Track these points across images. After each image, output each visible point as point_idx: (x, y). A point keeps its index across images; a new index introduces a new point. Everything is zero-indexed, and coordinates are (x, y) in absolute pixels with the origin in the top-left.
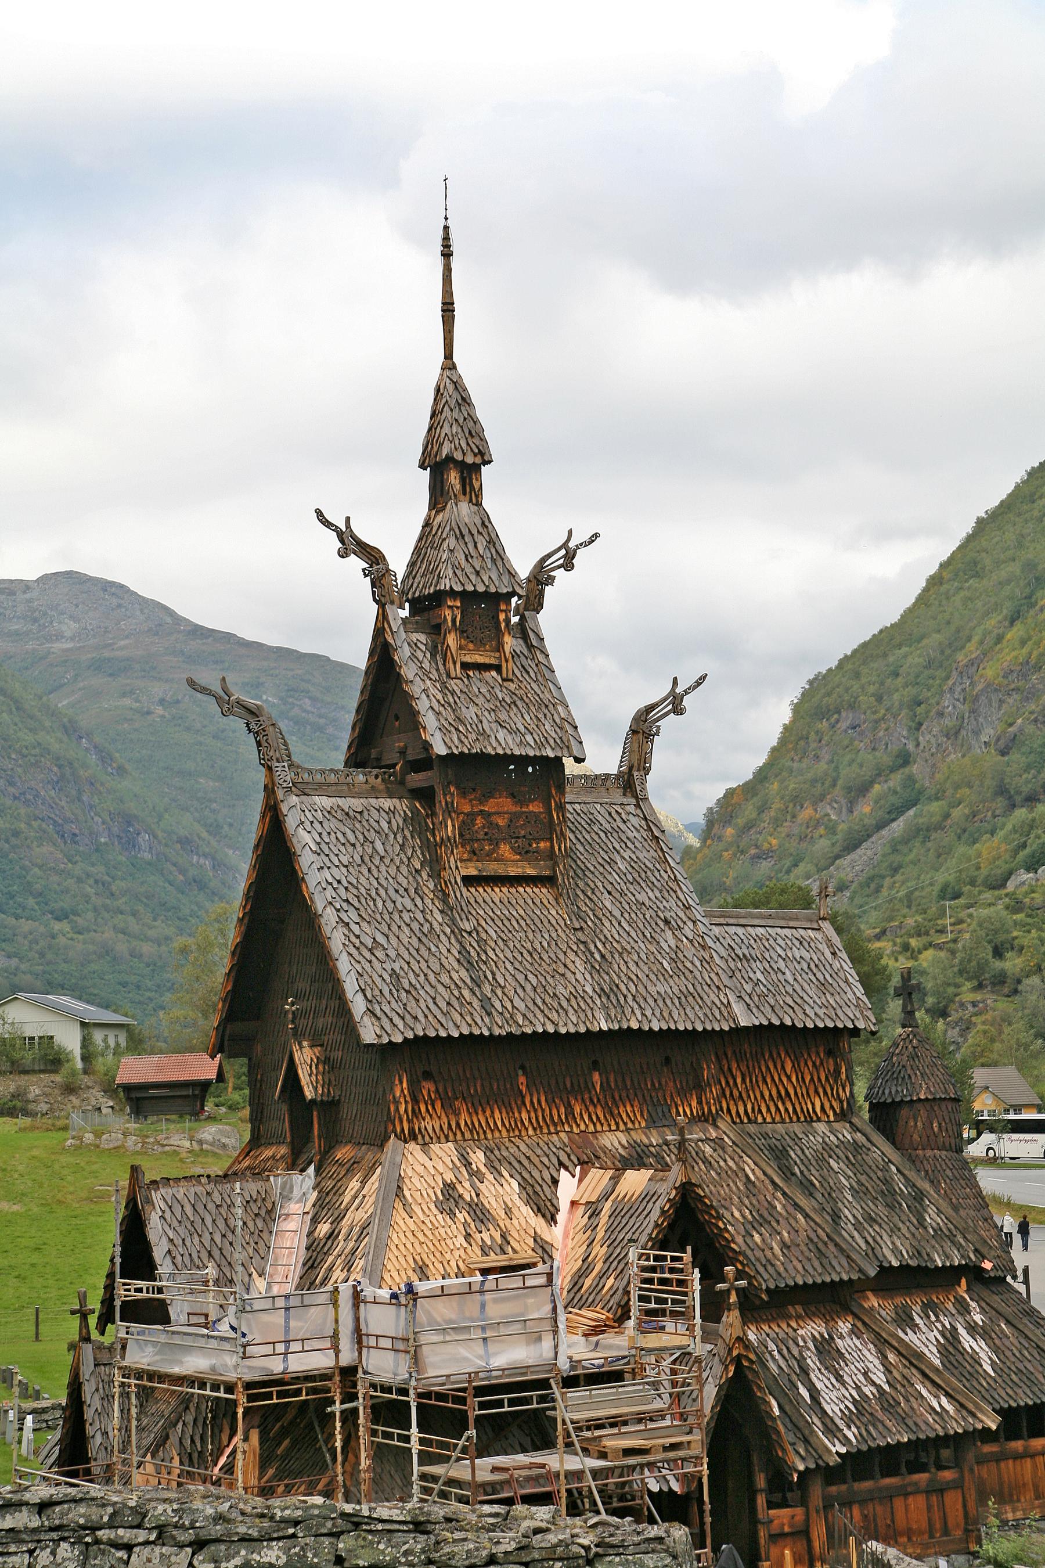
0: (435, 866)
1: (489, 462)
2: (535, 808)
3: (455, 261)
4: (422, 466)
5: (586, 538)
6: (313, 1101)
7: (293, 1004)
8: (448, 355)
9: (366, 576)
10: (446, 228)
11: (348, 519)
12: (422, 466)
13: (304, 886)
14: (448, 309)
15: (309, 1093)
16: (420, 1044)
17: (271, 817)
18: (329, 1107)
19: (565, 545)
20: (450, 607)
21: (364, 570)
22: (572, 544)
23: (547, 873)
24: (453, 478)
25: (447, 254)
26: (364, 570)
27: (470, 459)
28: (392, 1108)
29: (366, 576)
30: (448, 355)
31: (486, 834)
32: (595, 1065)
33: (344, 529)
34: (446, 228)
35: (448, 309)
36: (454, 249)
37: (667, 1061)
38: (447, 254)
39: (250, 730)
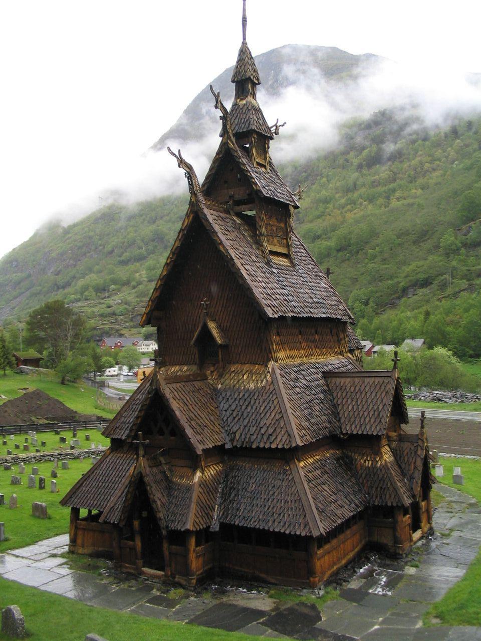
0: (259, 244)
1: (259, 84)
2: (282, 225)
4: (233, 81)
5: (282, 124)
6: (221, 345)
7: (205, 301)
8: (244, 39)
9: (221, 119)
13: (221, 247)
14: (244, 20)
15: (219, 341)
16: (282, 318)
17: (193, 217)
18: (224, 347)
19: (276, 125)
20: (254, 137)
22: (278, 125)
23: (287, 253)
28: (271, 347)
29: (221, 119)
30: (244, 39)
32: (316, 332)
35: (244, 20)
37: (331, 332)
39: (186, 176)
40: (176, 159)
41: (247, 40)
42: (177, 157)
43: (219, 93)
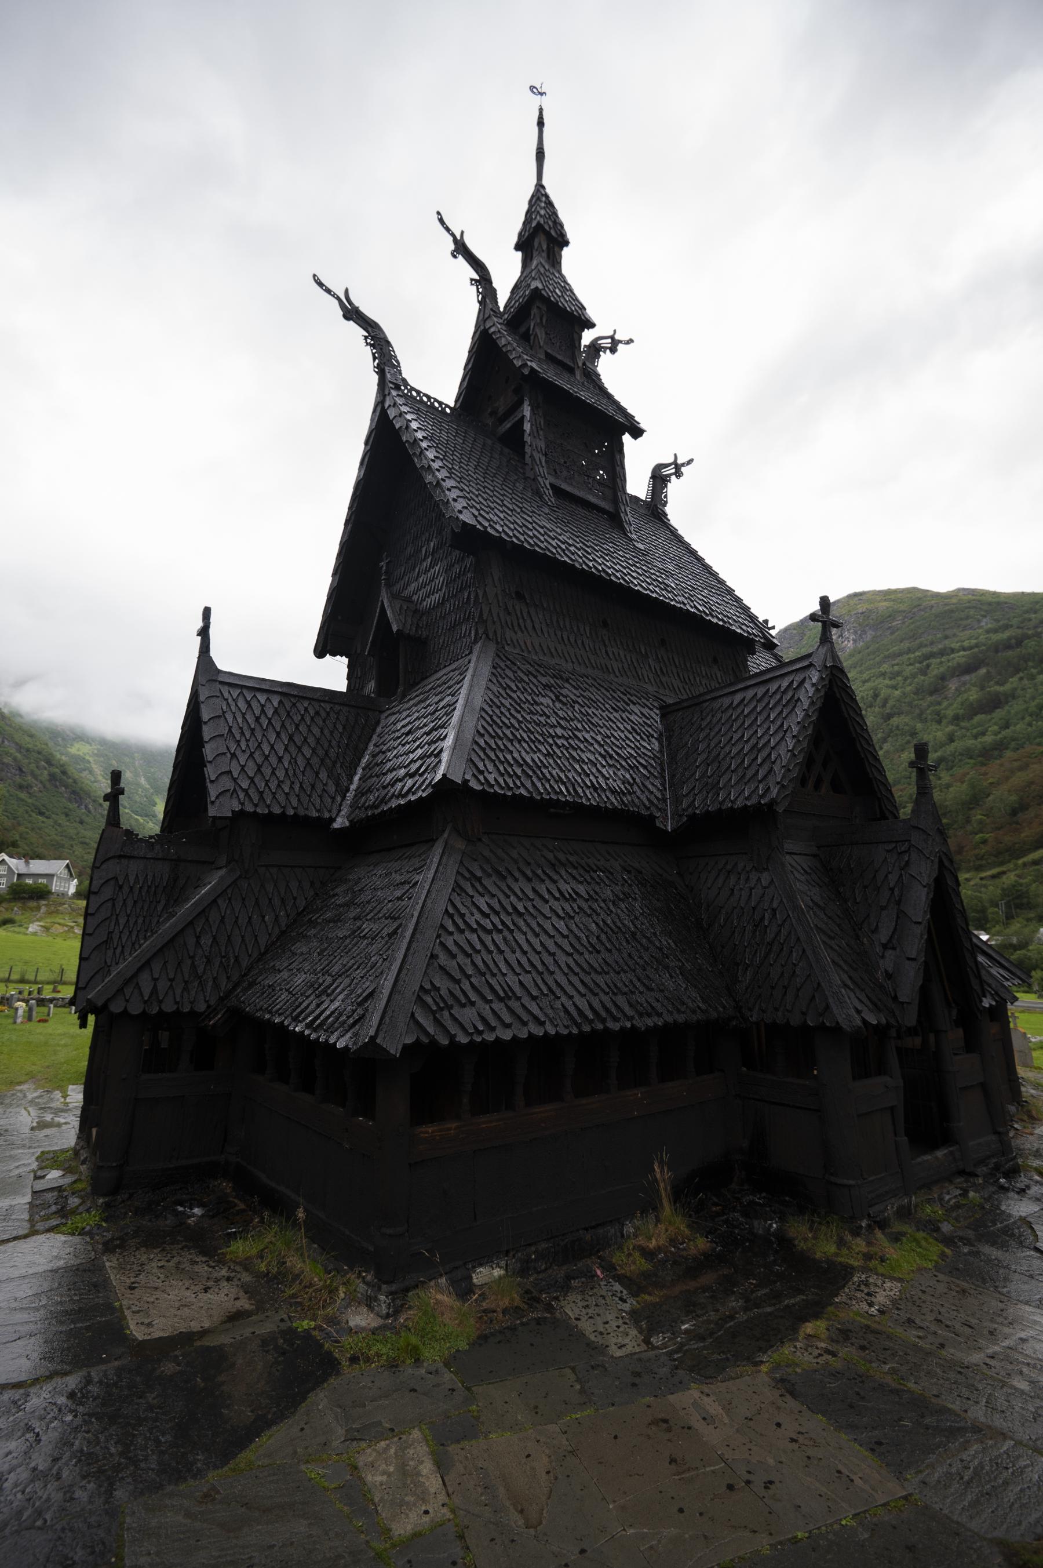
3: (545, 129)
4: (518, 247)
9: (472, 284)
10: (541, 110)
11: (462, 233)
12: (518, 247)
21: (472, 280)
24: (541, 241)
25: (541, 123)
26: (472, 280)
27: (553, 233)
29: (472, 284)
31: (565, 462)
33: (459, 238)
34: (541, 110)
36: (546, 121)
38: (541, 123)
39: (367, 344)
40: (336, 302)
41: (544, 182)
42: (338, 298)
43: (462, 233)
